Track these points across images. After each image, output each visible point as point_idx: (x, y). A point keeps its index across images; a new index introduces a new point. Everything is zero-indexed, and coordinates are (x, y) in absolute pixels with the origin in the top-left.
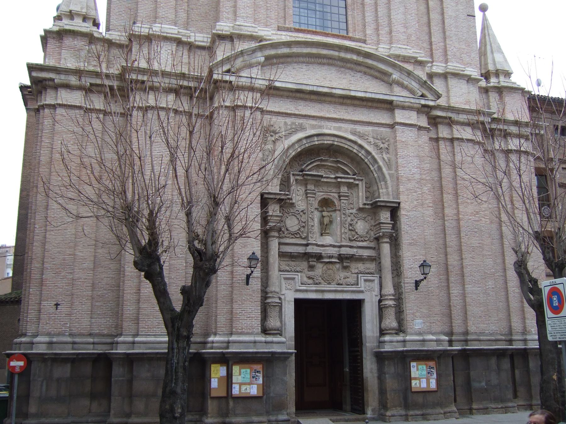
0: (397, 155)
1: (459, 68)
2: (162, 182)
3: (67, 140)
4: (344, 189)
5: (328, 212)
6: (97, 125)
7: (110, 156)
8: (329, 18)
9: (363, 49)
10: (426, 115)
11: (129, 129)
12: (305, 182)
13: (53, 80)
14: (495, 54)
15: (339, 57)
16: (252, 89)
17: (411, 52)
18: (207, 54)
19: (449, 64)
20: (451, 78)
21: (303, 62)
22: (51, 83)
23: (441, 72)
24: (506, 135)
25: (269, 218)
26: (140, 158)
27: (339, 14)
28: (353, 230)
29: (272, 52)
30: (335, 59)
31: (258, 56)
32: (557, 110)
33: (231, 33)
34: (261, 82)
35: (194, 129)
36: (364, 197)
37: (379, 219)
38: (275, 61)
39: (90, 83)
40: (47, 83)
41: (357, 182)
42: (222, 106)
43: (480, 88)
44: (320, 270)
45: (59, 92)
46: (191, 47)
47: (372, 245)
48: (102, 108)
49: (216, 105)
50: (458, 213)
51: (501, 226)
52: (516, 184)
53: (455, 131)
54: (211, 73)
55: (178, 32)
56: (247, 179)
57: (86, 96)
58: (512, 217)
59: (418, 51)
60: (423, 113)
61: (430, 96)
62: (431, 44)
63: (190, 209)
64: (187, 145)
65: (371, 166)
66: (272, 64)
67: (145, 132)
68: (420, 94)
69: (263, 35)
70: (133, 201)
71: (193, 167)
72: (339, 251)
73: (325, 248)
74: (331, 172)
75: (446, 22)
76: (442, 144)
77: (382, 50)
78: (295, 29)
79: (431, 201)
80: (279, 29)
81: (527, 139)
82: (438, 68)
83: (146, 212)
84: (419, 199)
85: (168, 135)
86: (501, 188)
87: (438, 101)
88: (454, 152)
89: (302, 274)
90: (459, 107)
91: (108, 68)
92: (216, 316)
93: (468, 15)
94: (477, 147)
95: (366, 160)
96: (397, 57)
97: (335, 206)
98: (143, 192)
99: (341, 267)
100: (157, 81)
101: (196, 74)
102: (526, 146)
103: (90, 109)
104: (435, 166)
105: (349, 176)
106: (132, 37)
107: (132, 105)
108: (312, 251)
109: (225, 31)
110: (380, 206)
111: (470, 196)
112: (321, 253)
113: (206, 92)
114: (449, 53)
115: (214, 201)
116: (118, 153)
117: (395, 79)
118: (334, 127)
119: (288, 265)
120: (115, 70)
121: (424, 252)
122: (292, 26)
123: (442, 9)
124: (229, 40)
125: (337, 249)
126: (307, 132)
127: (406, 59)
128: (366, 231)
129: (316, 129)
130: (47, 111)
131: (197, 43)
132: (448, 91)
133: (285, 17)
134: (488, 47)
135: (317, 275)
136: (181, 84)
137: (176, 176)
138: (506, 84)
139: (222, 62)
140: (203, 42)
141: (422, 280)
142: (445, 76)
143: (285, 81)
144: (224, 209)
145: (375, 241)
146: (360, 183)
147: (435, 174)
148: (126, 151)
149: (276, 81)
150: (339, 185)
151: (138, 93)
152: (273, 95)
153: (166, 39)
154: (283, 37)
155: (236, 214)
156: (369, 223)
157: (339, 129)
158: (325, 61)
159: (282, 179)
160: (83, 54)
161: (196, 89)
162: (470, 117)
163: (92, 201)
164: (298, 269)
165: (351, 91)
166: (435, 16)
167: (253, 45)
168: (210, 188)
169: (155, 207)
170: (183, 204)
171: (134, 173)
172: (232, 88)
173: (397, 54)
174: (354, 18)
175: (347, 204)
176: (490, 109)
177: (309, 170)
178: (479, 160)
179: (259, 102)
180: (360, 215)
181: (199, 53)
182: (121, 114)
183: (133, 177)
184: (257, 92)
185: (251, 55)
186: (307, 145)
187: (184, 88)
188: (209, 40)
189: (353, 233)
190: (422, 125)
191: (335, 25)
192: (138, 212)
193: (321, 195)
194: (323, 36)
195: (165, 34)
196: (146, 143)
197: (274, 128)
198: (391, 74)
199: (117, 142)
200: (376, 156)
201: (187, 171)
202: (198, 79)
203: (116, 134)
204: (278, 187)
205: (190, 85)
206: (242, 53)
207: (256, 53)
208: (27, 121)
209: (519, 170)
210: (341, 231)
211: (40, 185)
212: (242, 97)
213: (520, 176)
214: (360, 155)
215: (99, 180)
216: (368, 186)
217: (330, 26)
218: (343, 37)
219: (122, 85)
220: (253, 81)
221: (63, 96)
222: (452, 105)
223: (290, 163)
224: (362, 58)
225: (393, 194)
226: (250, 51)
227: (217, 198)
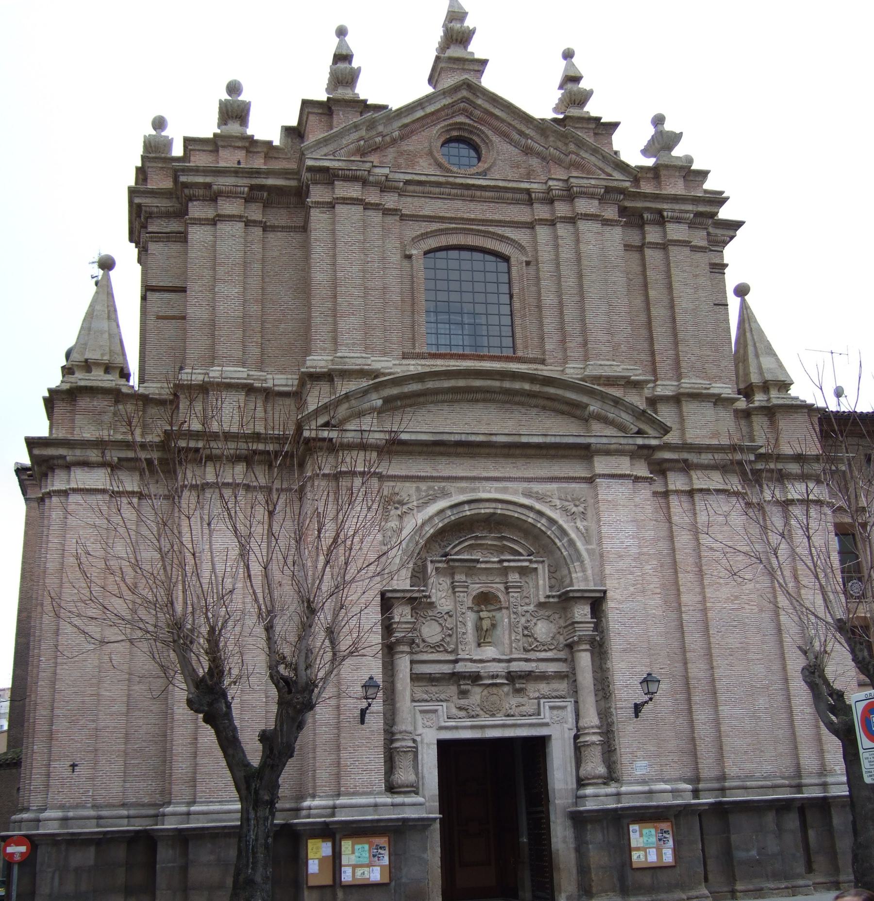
0: (599, 521)
1: (700, 386)
2: (228, 585)
3: (86, 538)
4: (514, 577)
5: (489, 611)
6: (129, 513)
7: (149, 555)
8: (485, 333)
9: (540, 373)
10: (645, 460)
11: (176, 515)
12: (451, 572)
13: (64, 457)
14: (761, 359)
15: (501, 388)
16: (363, 447)
17: (619, 369)
18: (293, 402)
19: (683, 381)
20: (687, 401)
21: (443, 401)
22: (60, 462)
23: (671, 394)
24: (782, 477)
25: (395, 626)
26: (194, 555)
27: (500, 325)
28: (529, 636)
29: (395, 391)
30: (495, 392)
31: (373, 399)
32: (868, 432)
33: (330, 369)
34: (377, 436)
35: (275, 508)
36: (547, 587)
37: (573, 617)
38: (399, 403)
39: (118, 458)
40: (56, 462)
41: (535, 566)
42: (318, 475)
43: (736, 411)
44: (478, 697)
45: (72, 473)
46: (269, 394)
47: (562, 655)
48: (136, 489)
49: (309, 474)
50: (704, 600)
51: (777, 615)
52: (802, 550)
53: (695, 481)
54: (299, 429)
55: (248, 375)
56: (358, 572)
57: (112, 475)
58: (796, 600)
59: (632, 367)
60: (640, 457)
61: (651, 432)
62: (653, 353)
63: (271, 621)
64: (266, 532)
65: (557, 541)
66: (396, 408)
67: (201, 518)
68: (635, 429)
69: (380, 367)
70: (185, 615)
71: (274, 562)
72: (508, 667)
73: (485, 664)
74: (492, 554)
75: (678, 318)
76: (674, 500)
77: (573, 371)
78: (430, 354)
79: (658, 585)
80: (405, 356)
81: (818, 482)
82: (666, 388)
83: (204, 630)
84: (637, 584)
85: (236, 520)
86: (777, 557)
87: (665, 438)
88: (694, 509)
89: (449, 704)
90: (701, 443)
91: (143, 435)
92: (315, 770)
93: (715, 304)
94: (734, 500)
95: (549, 533)
96: (597, 379)
97: (500, 602)
98: (199, 602)
99: (511, 691)
100: (217, 447)
101: (276, 432)
102: (818, 492)
103: (118, 492)
104: (664, 533)
105: (522, 558)
106: (180, 389)
107: (181, 483)
108: (463, 670)
109: (321, 367)
110: (574, 598)
111: (724, 573)
112: (479, 672)
113: (292, 456)
114: (683, 364)
115: (309, 607)
116: (160, 549)
117: (593, 412)
118: (496, 488)
119: (427, 692)
120: (154, 437)
121: (648, 660)
122: (425, 350)
123: (672, 300)
124: (326, 380)
125: (504, 665)
126: (452, 499)
127: (611, 381)
128: (551, 635)
129: (467, 493)
130: (55, 500)
131: (276, 388)
132: (682, 420)
133: (413, 338)
134: (750, 349)
135: (473, 705)
136: (254, 448)
137: (249, 576)
138: (781, 402)
139: (317, 412)
140: (286, 385)
141: (646, 702)
142: (677, 399)
143: (415, 430)
144: (323, 618)
145: (567, 650)
146: (540, 566)
147: (663, 545)
148: (172, 547)
149: (402, 432)
150: (505, 571)
151: (189, 466)
152: (397, 453)
153: (230, 387)
154: (412, 368)
155: (343, 624)
156: (555, 624)
157: (505, 490)
158: (479, 396)
159: (413, 569)
160: (107, 418)
161: (277, 454)
162: (718, 456)
163: (123, 620)
164: (443, 697)
165: (522, 437)
166: (659, 312)
167: (365, 384)
168: (302, 590)
169: (217, 621)
170: (260, 614)
171: (186, 576)
172: (332, 447)
173: (596, 375)
174: (524, 328)
175: (519, 599)
176: (753, 441)
177: (456, 554)
178: (737, 519)
179: (376, 465)
180: (541, 613)
181: (281, 403)
182: (165, 496)
183: (184, 582)
184: (371, 451)
185: (361, 399)
186: (453, 518)
187: (259, 453)
188: (296, 382)
189: (530, 640)
190: (639, 474)
191: (495, 342)
192: (192, 630)
193: (476, 588)
194: (474, 360)
195: (228, 380)
196: (202, 533)
197: (401, 496)
198: (587, 405)
199: (160, 535)
200: (565, 526)
201: (265, 568)
202: (280, 440)
203: (158, 523)
204: (408, 581)
205: (267, 449)
206: (347, 397)
207: (369, 396)
208: (27, 516)
209: (808, 529)
210: (510, 638)
211: (47, 601)
212: (348, 460)
213: (809, 538)
214: (539, 525)
215: (133, 590)
216: (552, 569)
217: (487, 345)
218: (508, 359)
219: (165, 457)
220: (366, 435)
221: (78, 477)
222: (689, 441)
223: (426, 546)
224: (538, 386)
225: (594, 579)
226: (360, 393)
227: (313, 602)
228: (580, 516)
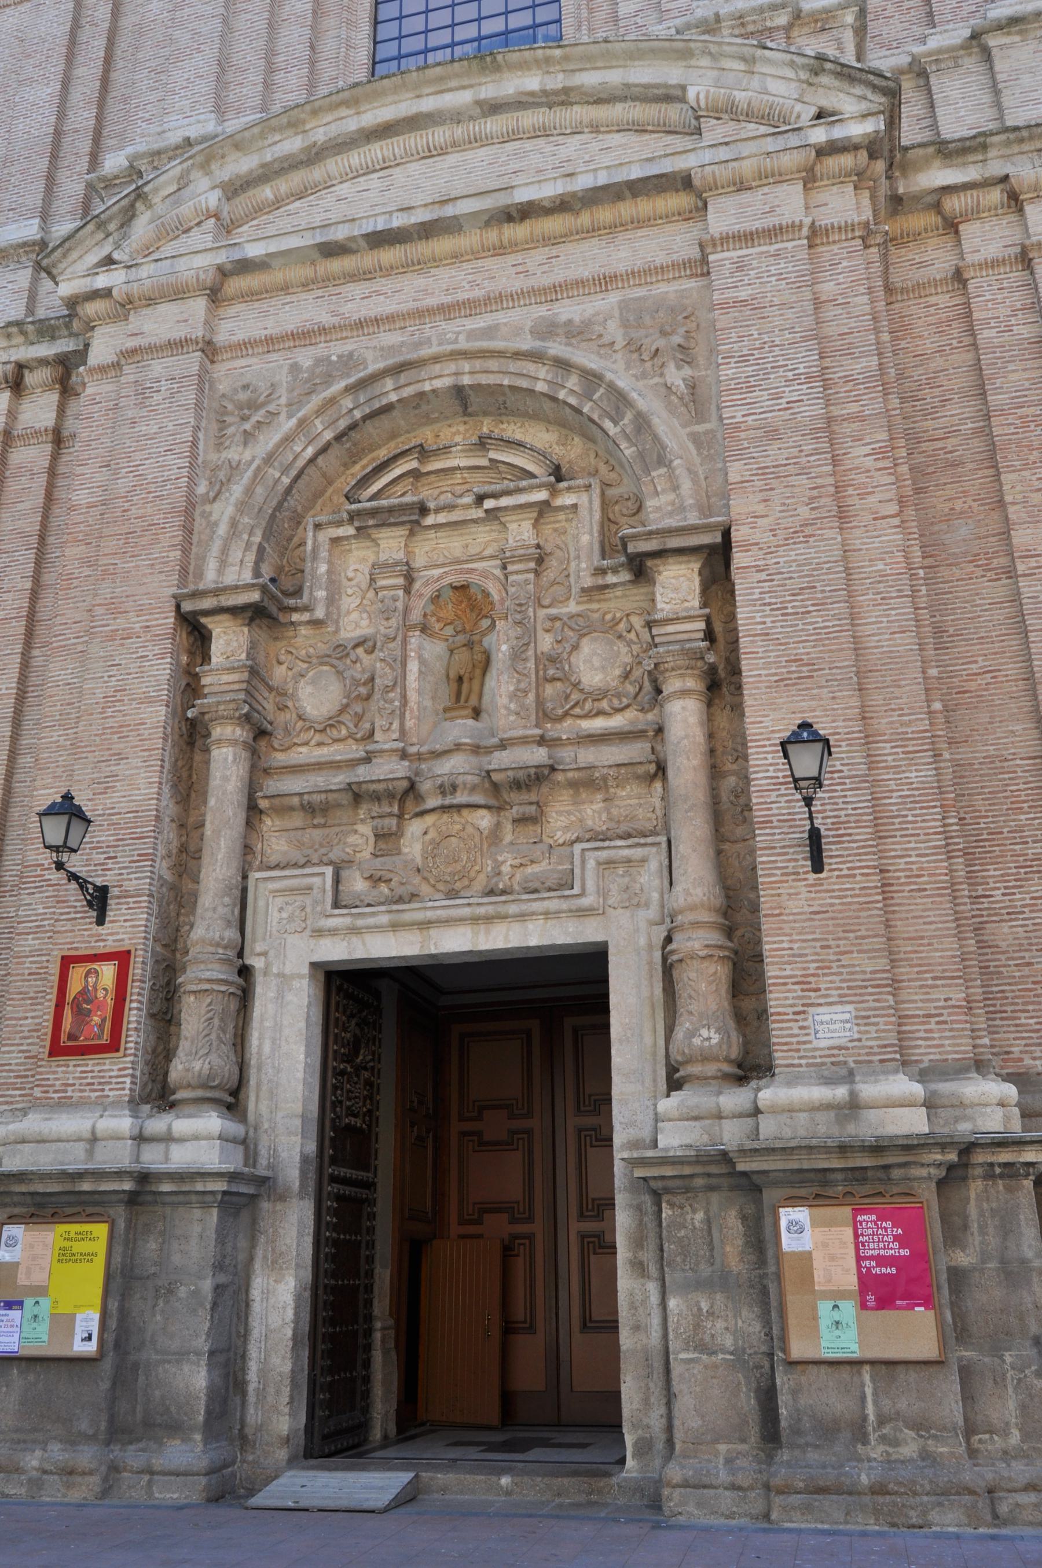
65: (608, 425)
214: (562, 395)
228: (674, 358)
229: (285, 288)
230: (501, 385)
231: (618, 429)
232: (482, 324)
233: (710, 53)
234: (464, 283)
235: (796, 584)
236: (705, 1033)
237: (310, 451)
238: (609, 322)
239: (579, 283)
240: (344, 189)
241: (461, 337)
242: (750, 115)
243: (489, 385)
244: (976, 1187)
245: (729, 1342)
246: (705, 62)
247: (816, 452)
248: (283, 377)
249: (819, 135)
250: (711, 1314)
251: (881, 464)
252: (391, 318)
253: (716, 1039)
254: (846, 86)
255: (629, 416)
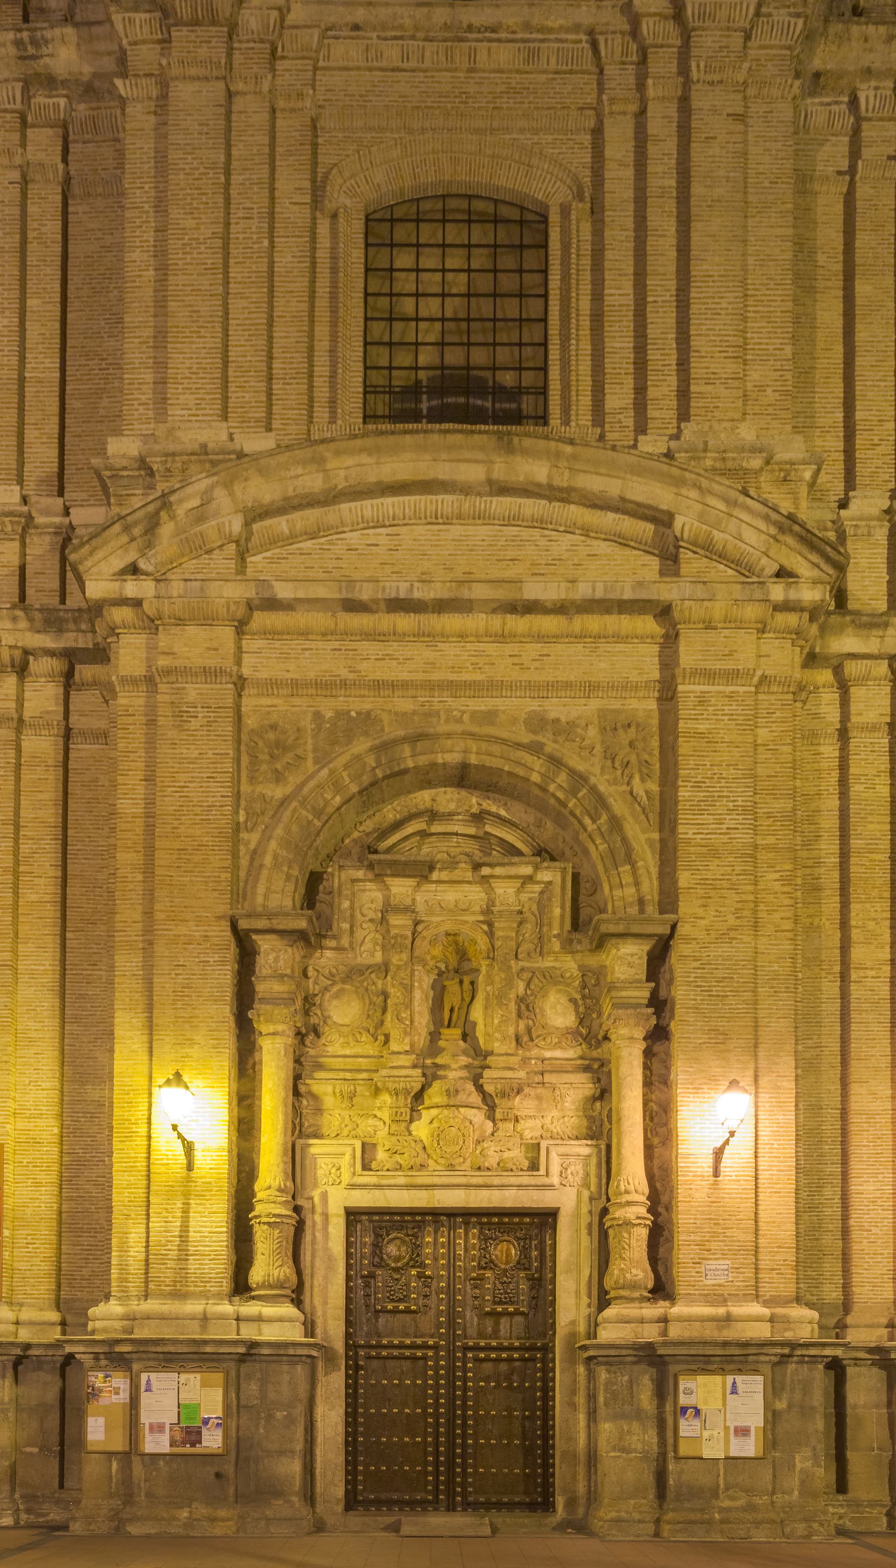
65: (587, 821)
229: (305, 634)
230: (502, 770)
231: (595, 827)
232: (483, 708)
233: (700, 488)
234: (468, 665)
235: (720, 974)
236: (634, 1271)
237: (338, 799)
238: (590, 727)
239: (568, 685)
240: (353, 538)
241: (466, 717)
242: (722, 556)
243: (491, 768)
244: (791, 1367)
245: (639, 1446)
246: (693, 494)
247: (744, 873)
248: (307, 724)
249: (778, 592)
250: (629, 1432)
251: (785, 889)
252: (405, 685)
253: (641, 1275)
254: (805, 551)
255: (604, 818)
